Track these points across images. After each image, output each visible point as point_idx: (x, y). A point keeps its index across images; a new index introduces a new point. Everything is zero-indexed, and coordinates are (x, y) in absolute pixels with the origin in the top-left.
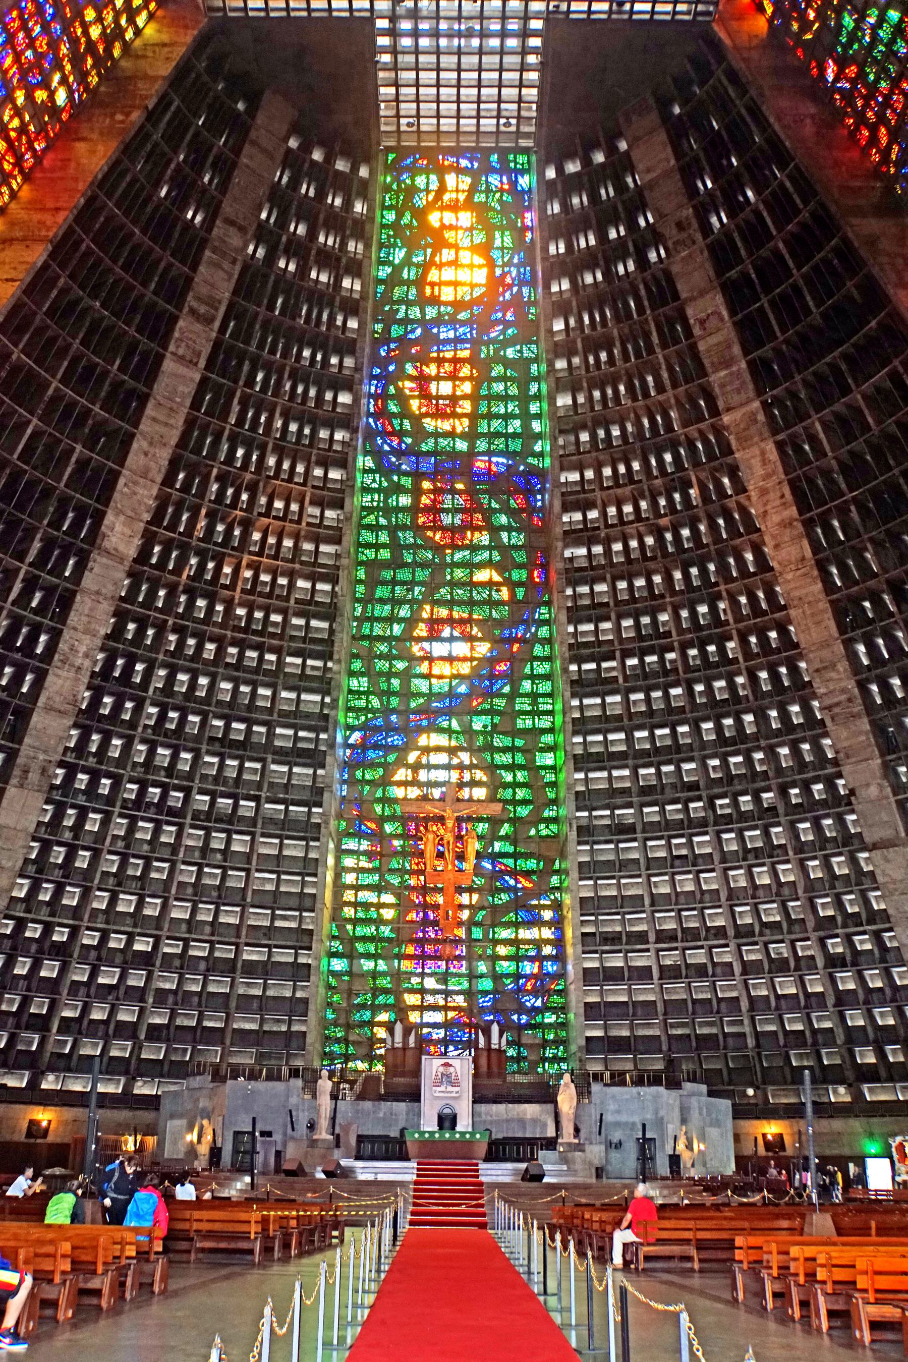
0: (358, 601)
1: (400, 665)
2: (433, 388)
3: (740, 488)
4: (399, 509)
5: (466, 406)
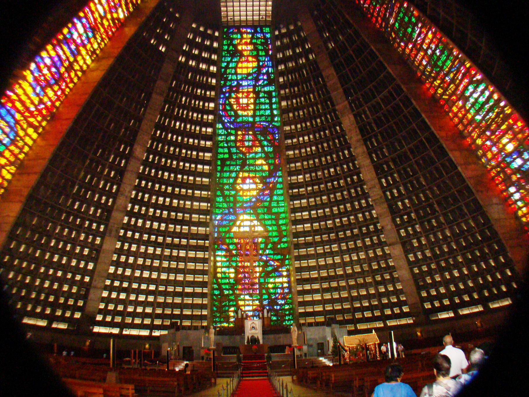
0: (219, 172)
1: (233, 193)
2: (241, 101)
5: (252, 107)
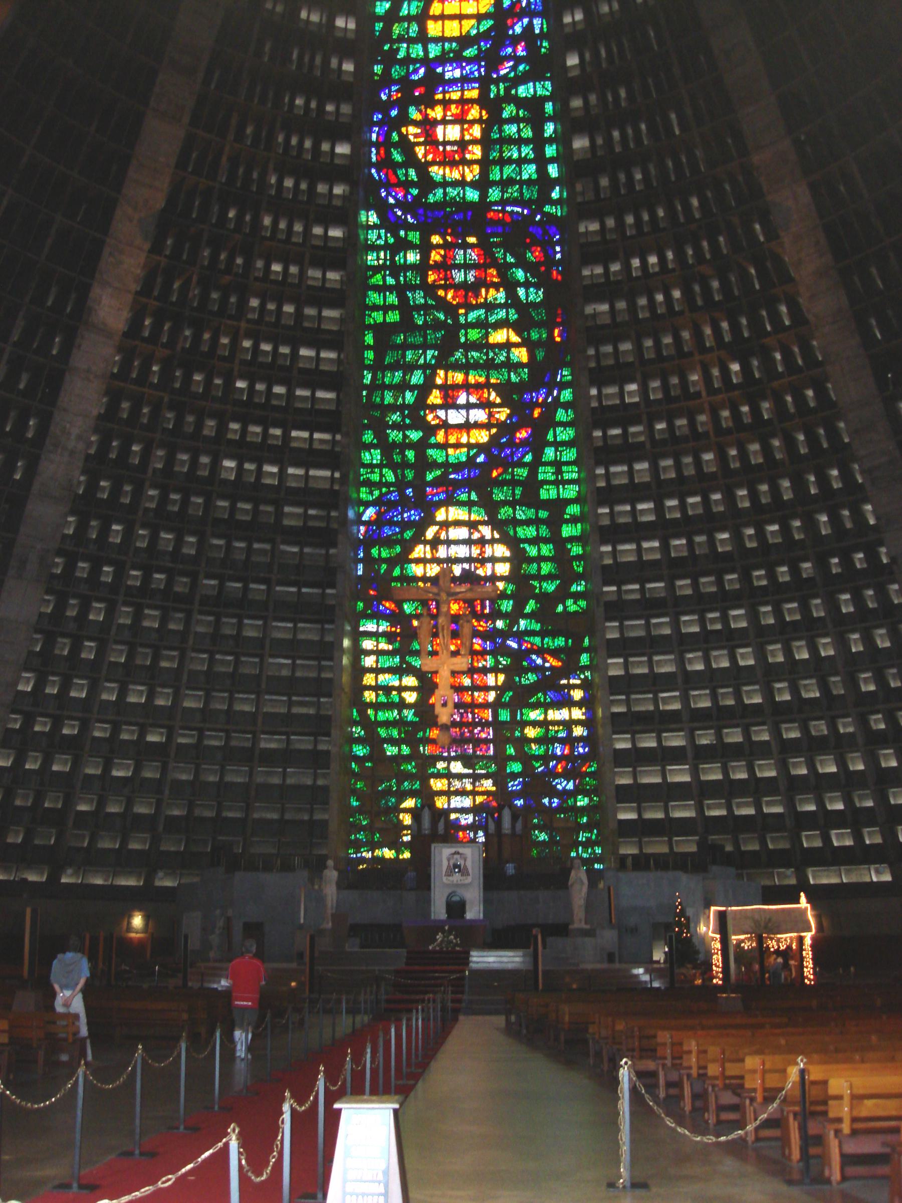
0: (369, 368)
1: (415, 435)
3: (772, 234)
4: (406, 267)
5: (476, 152)
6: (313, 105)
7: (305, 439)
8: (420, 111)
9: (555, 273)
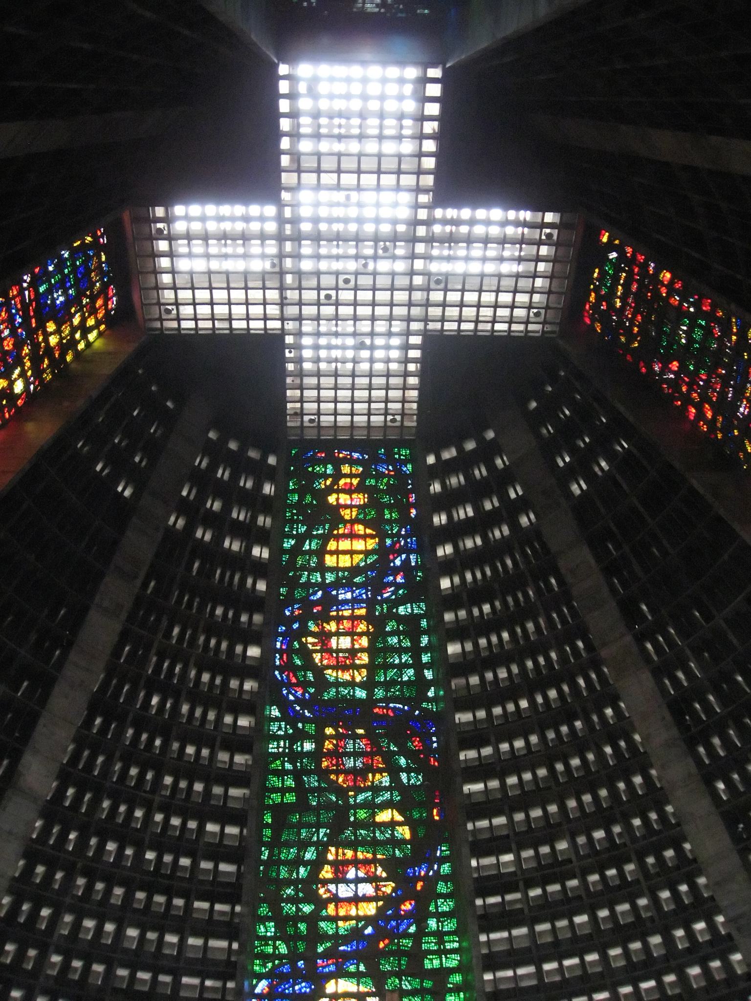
0: (265, 844)
1: (307, 909)
2: (333, 642)
4: (303, 754)
5: (364, 658)
6: (231, 614)
7: (205, 910)
8: (317, 625)
9: (432, 759)
